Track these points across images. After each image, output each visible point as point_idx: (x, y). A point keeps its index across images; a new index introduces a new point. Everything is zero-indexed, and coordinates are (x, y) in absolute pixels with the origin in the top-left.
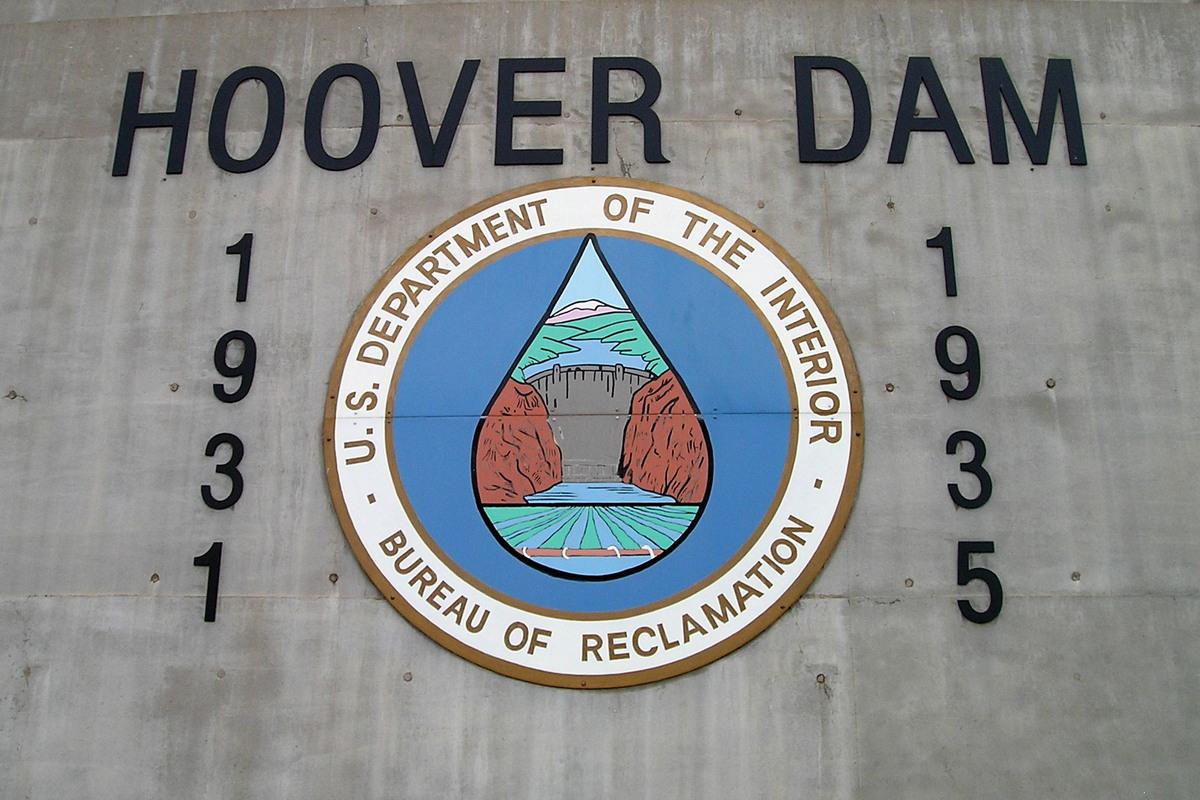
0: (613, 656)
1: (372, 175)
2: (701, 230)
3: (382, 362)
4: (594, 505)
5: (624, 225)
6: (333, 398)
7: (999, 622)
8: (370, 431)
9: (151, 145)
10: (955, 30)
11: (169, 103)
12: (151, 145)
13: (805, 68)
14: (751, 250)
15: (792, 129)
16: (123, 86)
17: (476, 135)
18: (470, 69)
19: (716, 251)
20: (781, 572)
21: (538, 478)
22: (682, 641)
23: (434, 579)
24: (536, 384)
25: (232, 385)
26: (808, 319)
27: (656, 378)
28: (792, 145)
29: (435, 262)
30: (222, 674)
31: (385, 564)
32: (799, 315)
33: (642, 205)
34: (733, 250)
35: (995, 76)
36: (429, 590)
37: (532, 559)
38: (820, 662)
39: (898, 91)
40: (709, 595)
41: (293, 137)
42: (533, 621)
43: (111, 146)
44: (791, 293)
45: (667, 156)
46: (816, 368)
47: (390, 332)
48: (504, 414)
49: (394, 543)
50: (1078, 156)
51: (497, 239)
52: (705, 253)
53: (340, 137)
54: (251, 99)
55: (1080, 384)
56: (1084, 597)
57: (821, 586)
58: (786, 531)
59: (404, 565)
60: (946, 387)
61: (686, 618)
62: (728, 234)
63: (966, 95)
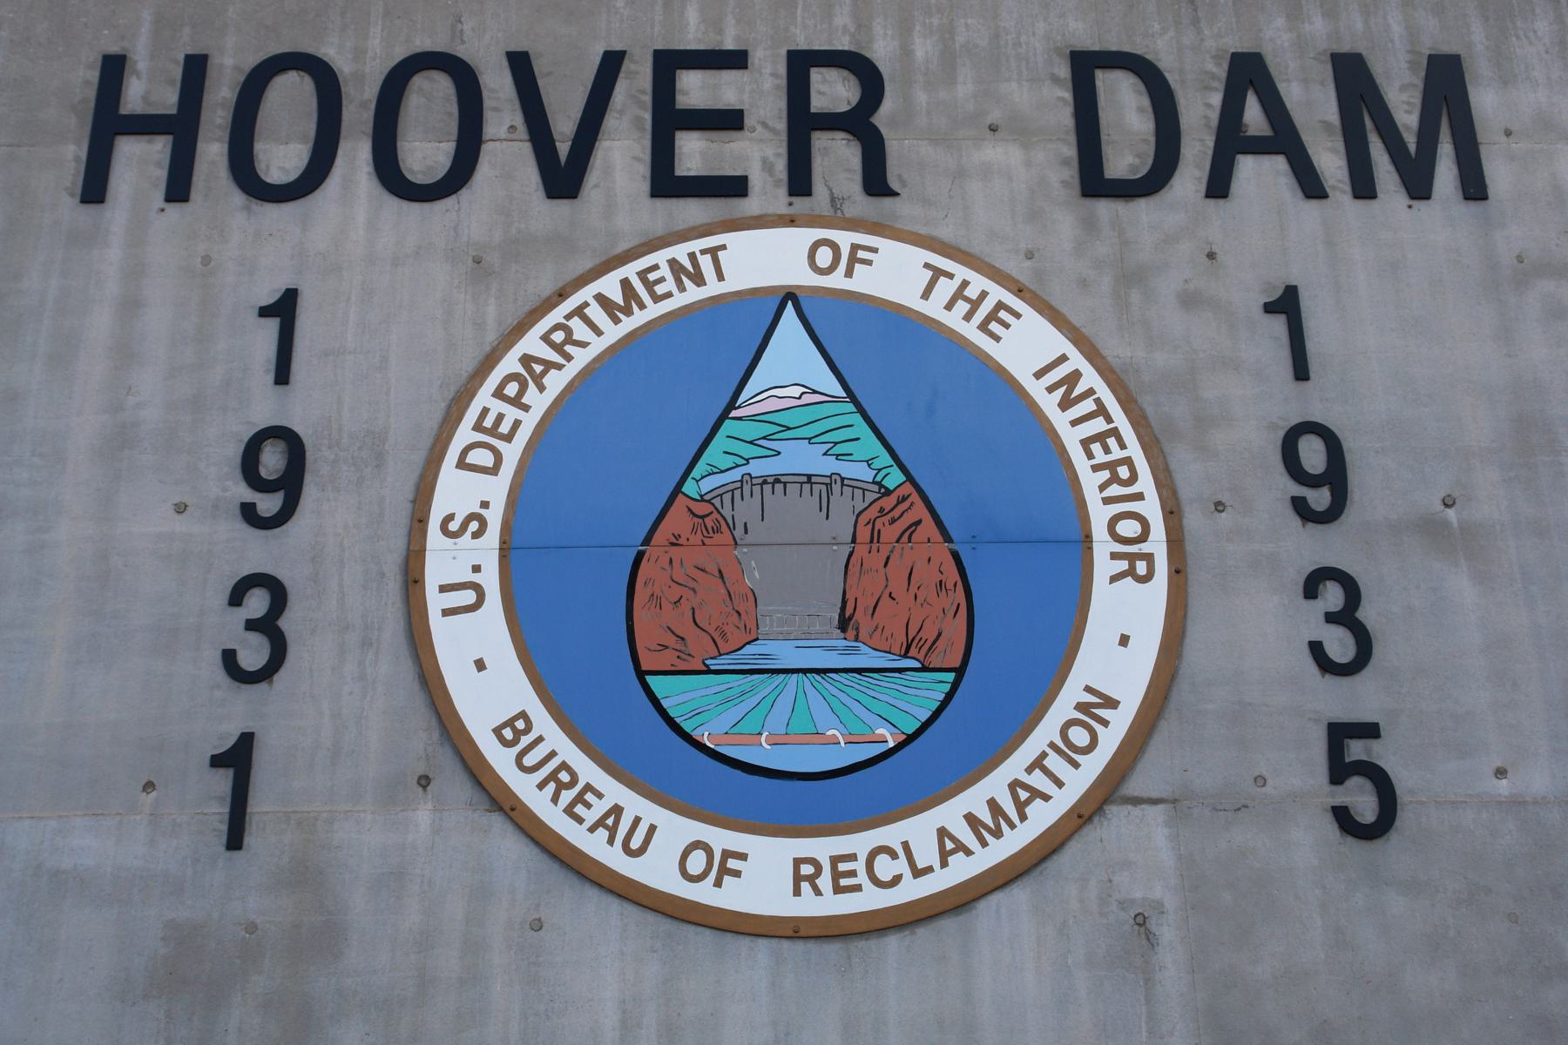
0: (838, 890)
1: (474, 209)
2: (945, 288)
3: (494, 470)
4: (805, 671)
5: (837, 281)
6: (419, 521)
7: (1394, 838)
8: (477, 569)
9: (139, 162)
10: (1295, 14)
11: (167, 100)
12: (139, 162)
13: (1085, 67)
14: (1018, 316)
15: (1070, 151)
16: (94, 75)
17: (622, 154)
18: (612, 64)
19: (968, 317)
20: (1076, 765)
21: (723, 634)
22: (937, 866)
24: (717, 502)
25: (269, 504)
26: (1101, 411)
27: (888, 492)
28: (1071, 173)
29: (568, 331)
30: (252, 928)
31: (501, 760)
32: (1088, 406)
33: (861, 254)
34: (992, 316)
35: (1353, 78)
36: (567, 796)
37: (719, 749)
38: (1138, 895)
39: (1216, 99)
40: (974, 799)
41: (355, 154)
42: (721, 839)
43: (77, 159)
44: (1075, 376)
45: (894, 184)
46: (1114, 478)
47: (504, 428)
48: (673, 544)
49: (514, 729)
50: (1474, 187)
51: (657, 299)
52: (953, 319)
53: (425, 154)
54: (290, 98)
55: (1490, 500)
56: (1515, 803)
57: (1136, 785)
59: (529, 761)
60: (1299, 505)
61: (943, 833)
62: (984, 295)
63: (1313, 104)
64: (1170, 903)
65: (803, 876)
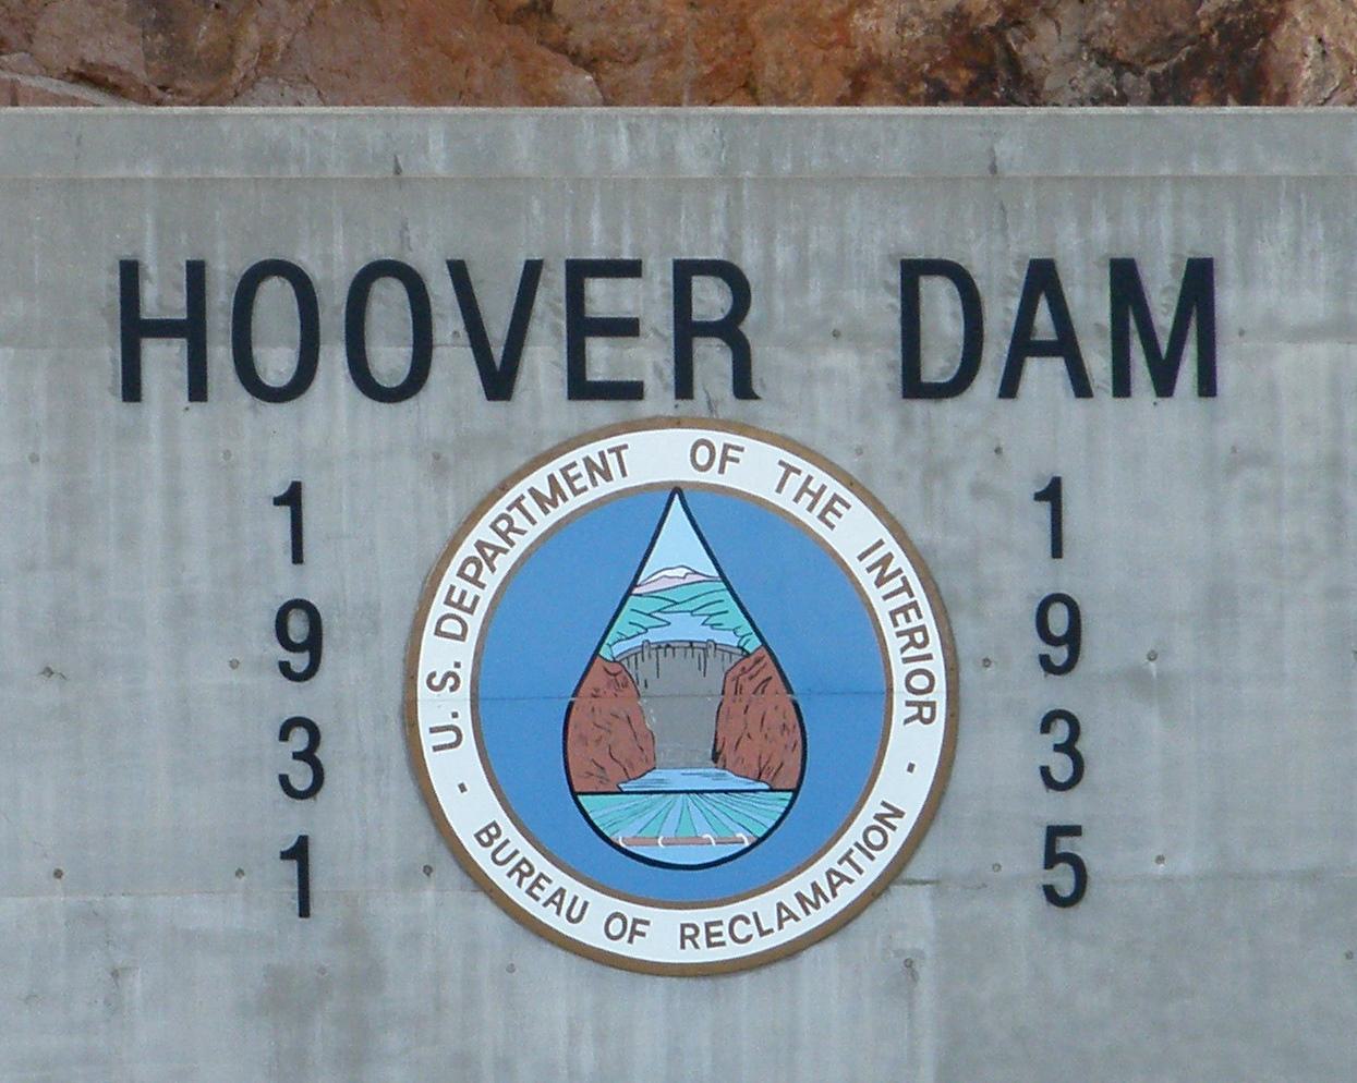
0: (710, 945)
2: (795, 482)
3: (462, 638)
4: (688, 792)
5: (711, 477)
7: (1082, 906)
8: (455, 715)
9: (163, 360)
10: (1085, 219)
11: (178, 308)
12: (163, 360)
13: (913, 272)
14: (848, 506)
15: (896, 356)
16: (116, 279)
17: (544, 360)
18: (533, 271)
19: (810, 509)
21: (631, 765)
22: (776, 928)
23: (532, 871)
24: (625, 663)
26: (906, 587)
27: (748, 655)
28: (896, 377)
29: (511, 521)
30: (322, 970)
31: (481, 856)
33: (731, 453)
34: (829, 508)
35: (1125, 280)
36: (528, 881)
37: (628, 848)
38: (908, 946)
39: (1015, 304)
40: (801, 883)
42: (632, 911)
43: (114, 361)
44: (888, 559)
45: (757, 389)
46: (913, 643)
47: (467, 603)
48: (595, 697)
49: (489, 834)
50: (1207, 385)
51: (576, 492)
52: (799, 511)
53: (390, 358)
54: (275, 302)
55: (1184, 652)
56: (1167, 880)
57: (914, 870)
58: (879, 817)
59: (500, 857)
60: (1045, 661)
61: (780, 906)
62: (823, 488)
63: (1090, 304)
64: (928, 954)
65: (686, 936)
